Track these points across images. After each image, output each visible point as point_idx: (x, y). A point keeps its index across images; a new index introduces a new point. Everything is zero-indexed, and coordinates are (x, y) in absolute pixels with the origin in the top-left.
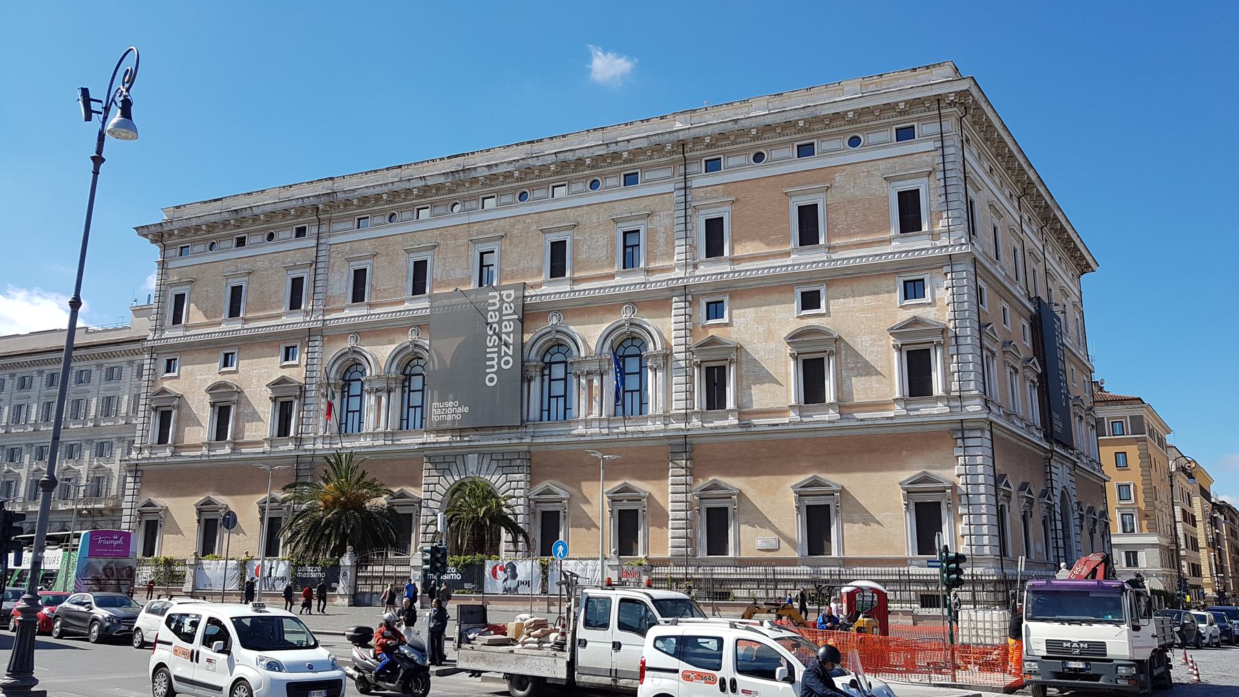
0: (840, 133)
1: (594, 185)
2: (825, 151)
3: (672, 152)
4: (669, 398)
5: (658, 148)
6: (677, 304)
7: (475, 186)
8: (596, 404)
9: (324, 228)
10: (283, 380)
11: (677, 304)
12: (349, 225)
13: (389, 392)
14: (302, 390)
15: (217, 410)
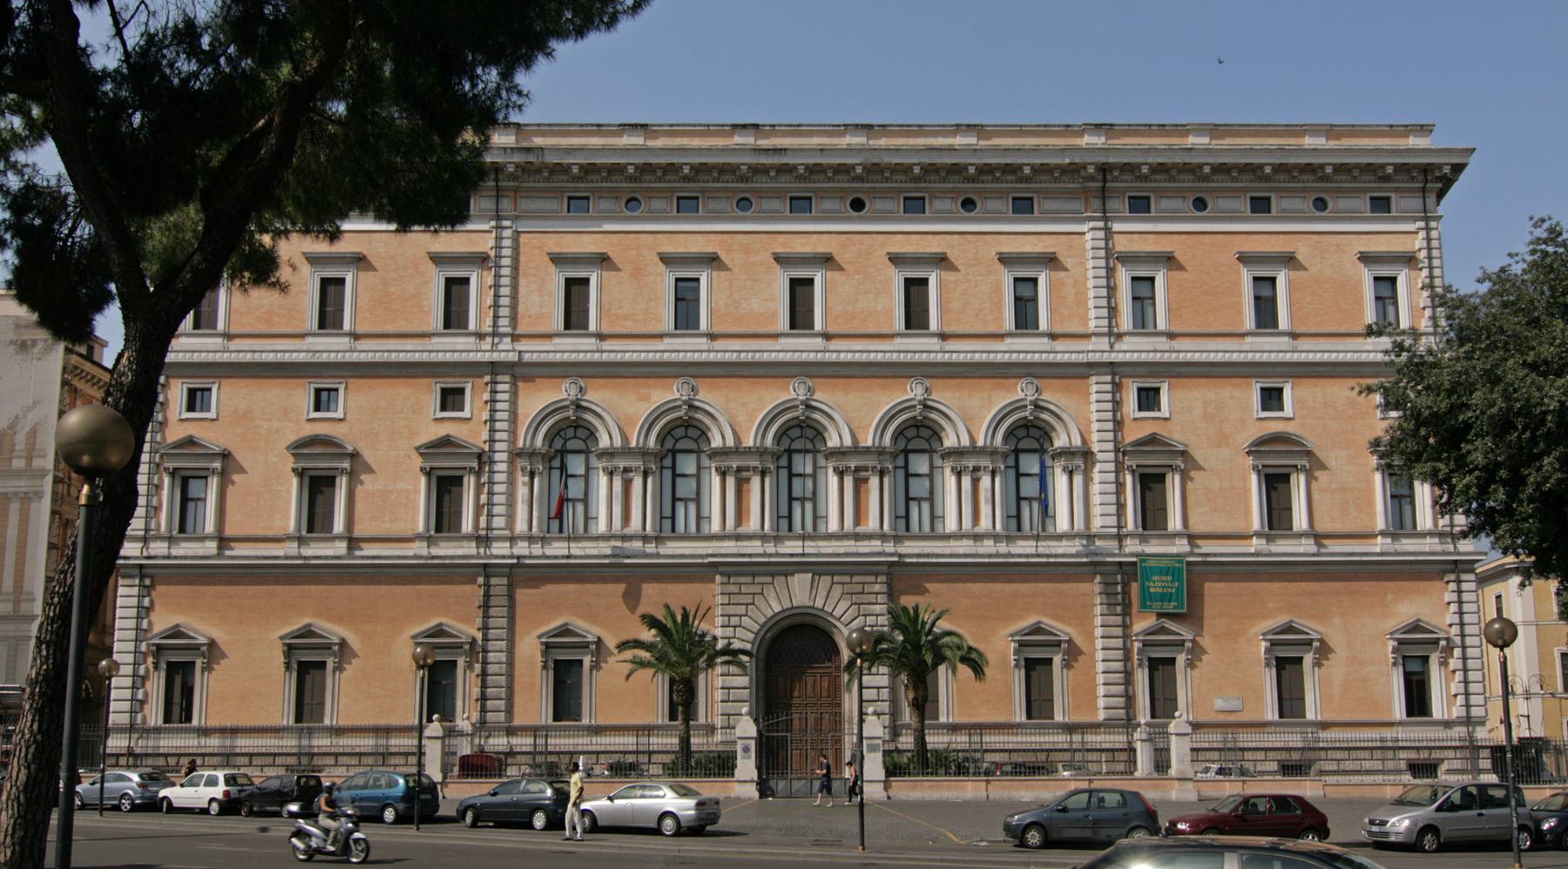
0: (1304, 190)
1: (968, 204)
2: (1284, 211)
3: (1091, 178)
4: (1085, 506)
5: (1073, 170)
6: (1097, 387)
7: (783, 178)
8: (985, 509)
9: (506, 204)
10: (446, 442)
11: (1097, 387)
12: (551, 205)
13: (645, 475)
14: (484, 459)
15: (306, 482)
